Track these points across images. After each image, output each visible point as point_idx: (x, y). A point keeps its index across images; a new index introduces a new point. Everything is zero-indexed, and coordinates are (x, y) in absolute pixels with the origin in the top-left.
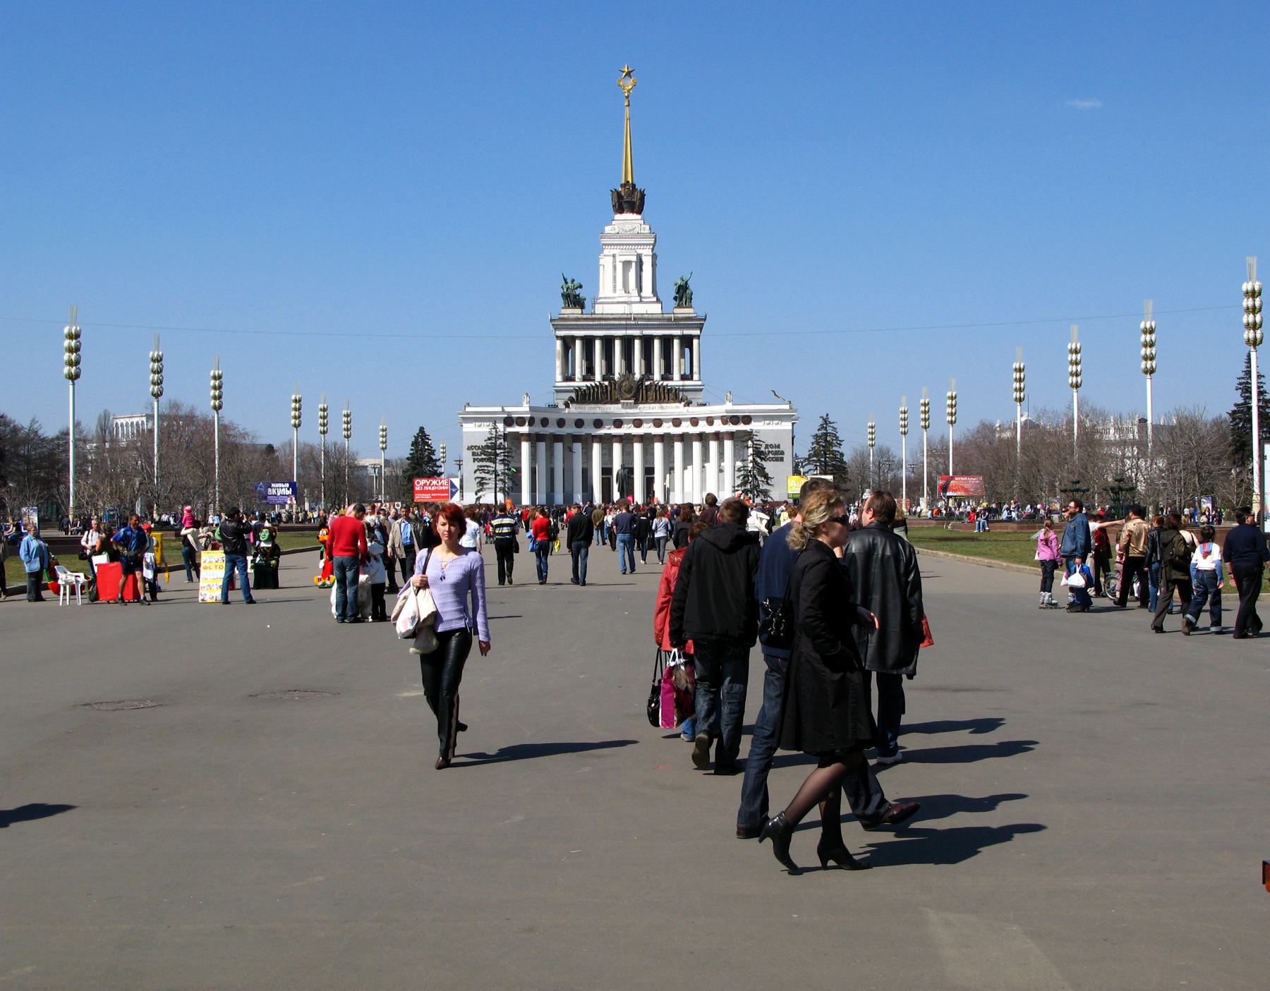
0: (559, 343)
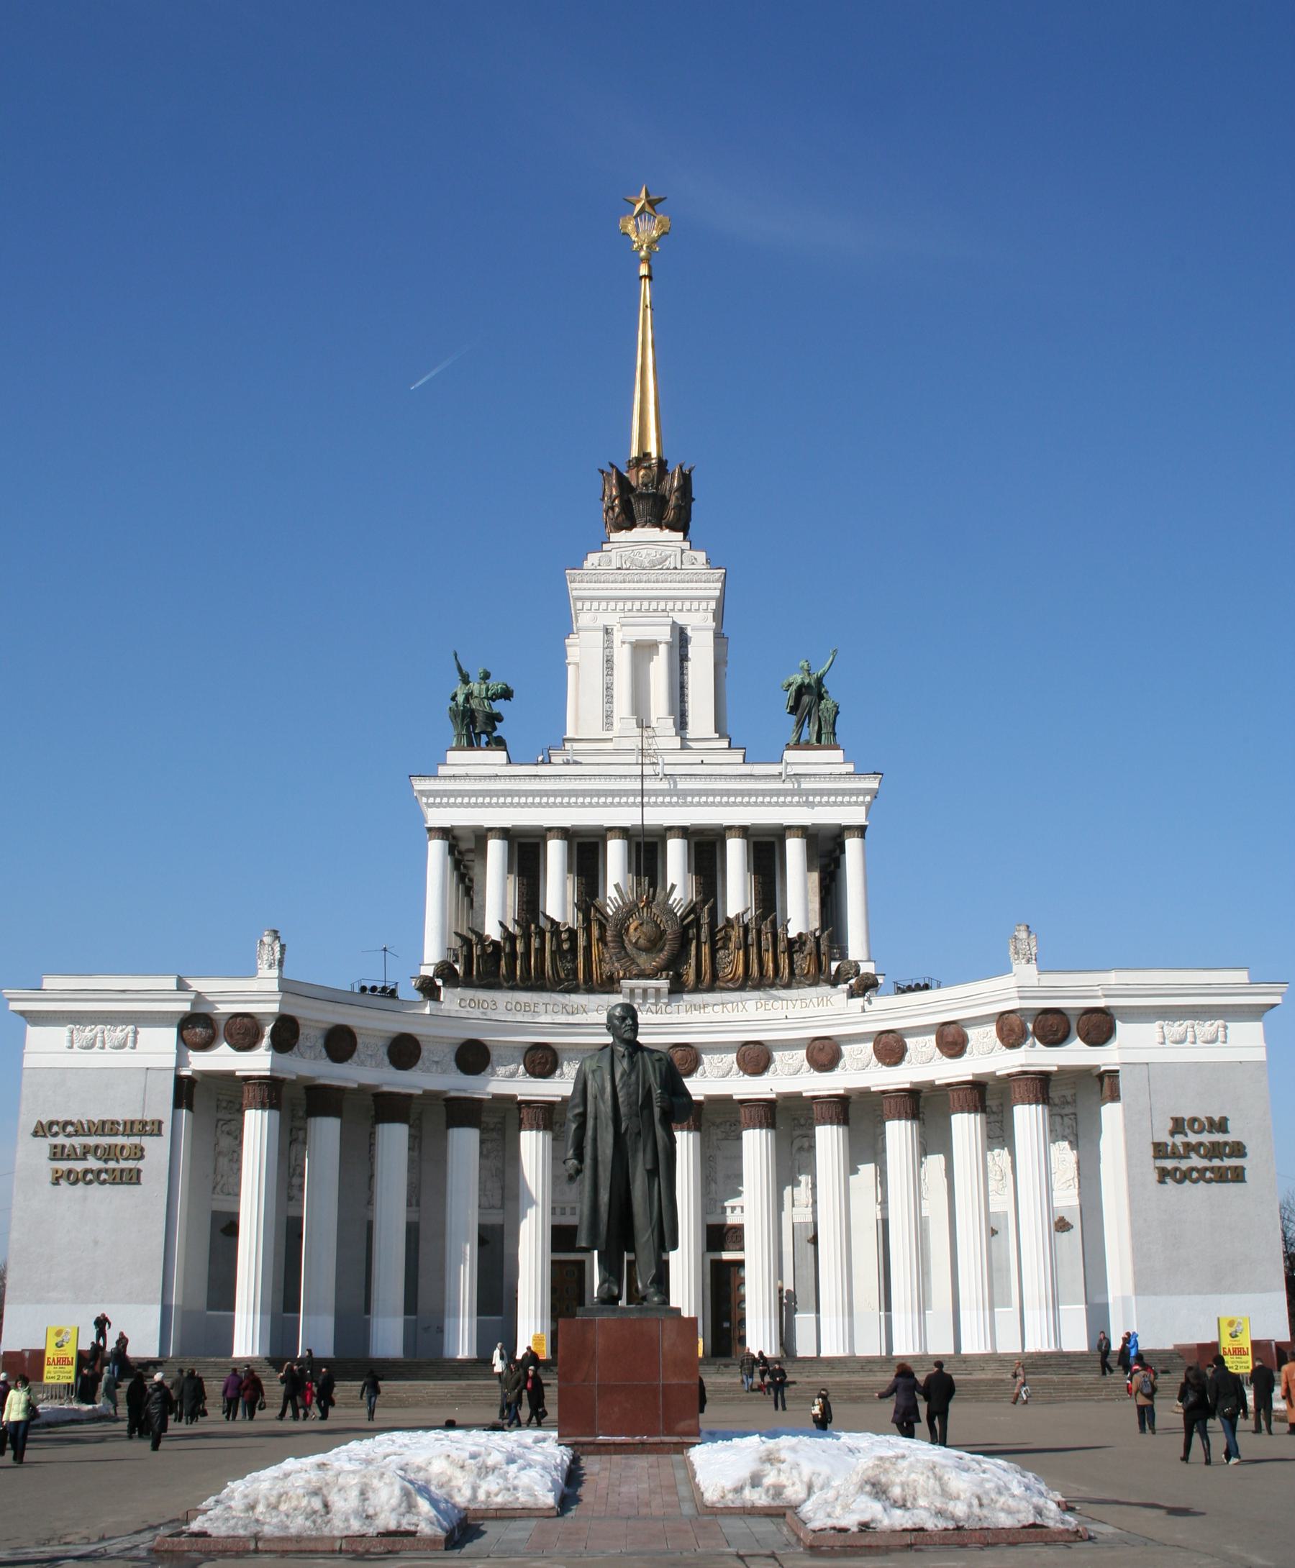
0: (436, 849)
